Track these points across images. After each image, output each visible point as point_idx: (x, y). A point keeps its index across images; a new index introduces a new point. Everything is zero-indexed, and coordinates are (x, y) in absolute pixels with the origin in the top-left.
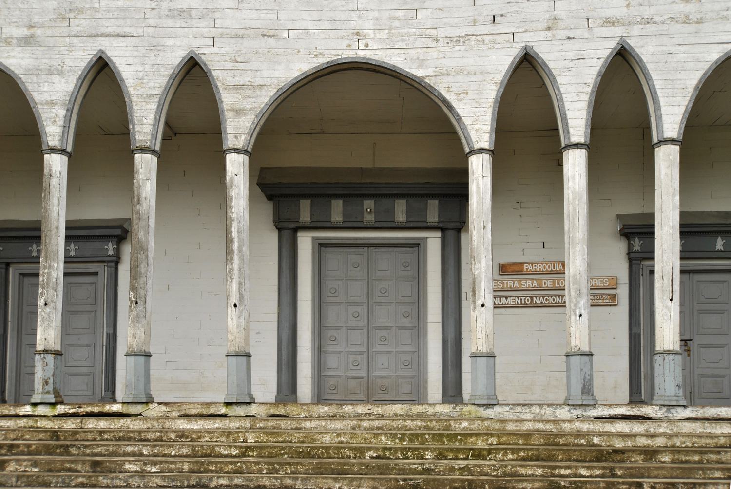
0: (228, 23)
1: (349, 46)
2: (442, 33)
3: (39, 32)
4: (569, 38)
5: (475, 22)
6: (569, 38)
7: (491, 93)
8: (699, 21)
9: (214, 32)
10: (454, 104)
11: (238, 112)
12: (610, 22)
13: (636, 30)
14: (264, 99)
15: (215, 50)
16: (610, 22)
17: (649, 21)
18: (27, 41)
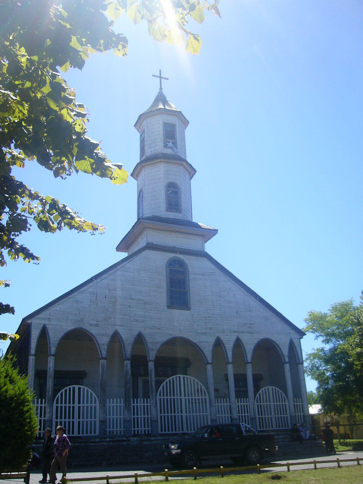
1: (178, 333)
2: (199, 331)
3: (100, 323)
4: (227, 335)
5: (206, 329)
6: (227, 335)
7: (211, 348)
8: (253, 333)
10: (204, 351)
11: (153, 350)
12: (235, 332)
13: (240, 334)
14: (158, 346)
15: (145, 332)
16: (235, 332)
18: (96, 325)
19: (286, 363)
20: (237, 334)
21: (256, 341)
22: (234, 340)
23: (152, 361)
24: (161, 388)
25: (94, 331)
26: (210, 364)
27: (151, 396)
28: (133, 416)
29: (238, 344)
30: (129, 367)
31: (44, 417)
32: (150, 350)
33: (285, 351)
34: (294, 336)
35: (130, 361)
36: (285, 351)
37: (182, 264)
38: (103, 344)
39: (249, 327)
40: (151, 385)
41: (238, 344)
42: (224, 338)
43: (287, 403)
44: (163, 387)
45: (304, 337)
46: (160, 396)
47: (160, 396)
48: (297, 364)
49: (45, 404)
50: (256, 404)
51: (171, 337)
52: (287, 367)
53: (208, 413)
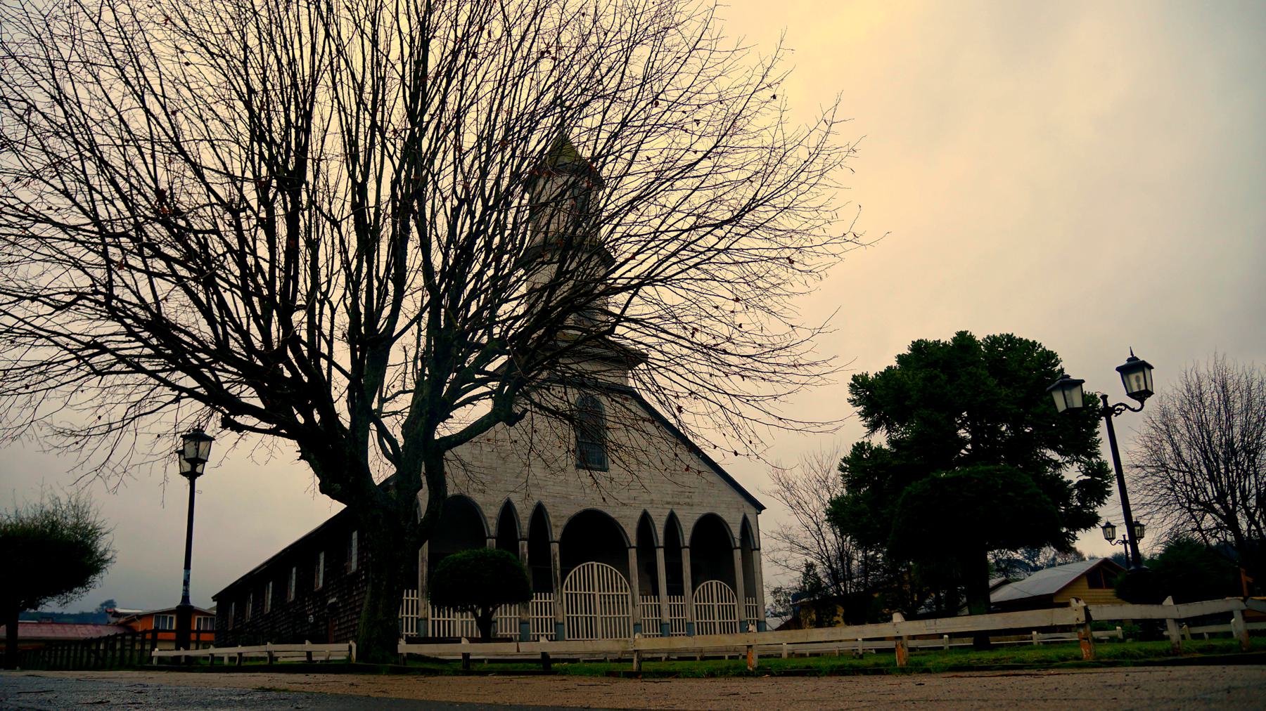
0: (551, 491)
5: (629, 499)
7: (635, 526)
9: (546, 494)
11: (557, 526)
12: (668, 503)
13: (675, 507)
14: (565, 522)
16: (668, 503)
17: (679, 504)
19: (737, 548)
20: (670, 506)
21: (697, 517)
22: (667, 514)
23: (557, 542)
24: (568, 579)
25: (478, 498)
26: (634, 547)
27: (555, 591)
28: (531, 616)
29: (672, 523)
30: (526, 550)
31: (417, 614)
32: (553, 527)
33: (736, 531)
34: (751, 511)
35: (526, 542)
36: (736, 531)
37: (597, 404)
38: (491, 518)
39: (688, 497)
40: (555, 573)
41: (672, 523)
42: (652, 513)
43: (736, 603)
44: (571, 578)
45: (763, 511)
46: (567, 590)
47: (567, 590)
48: (752, 550)
49: (417, 596)
50: (694, 603)
51: (582, 509)
52: (738, 554)
53: (630, 615)
